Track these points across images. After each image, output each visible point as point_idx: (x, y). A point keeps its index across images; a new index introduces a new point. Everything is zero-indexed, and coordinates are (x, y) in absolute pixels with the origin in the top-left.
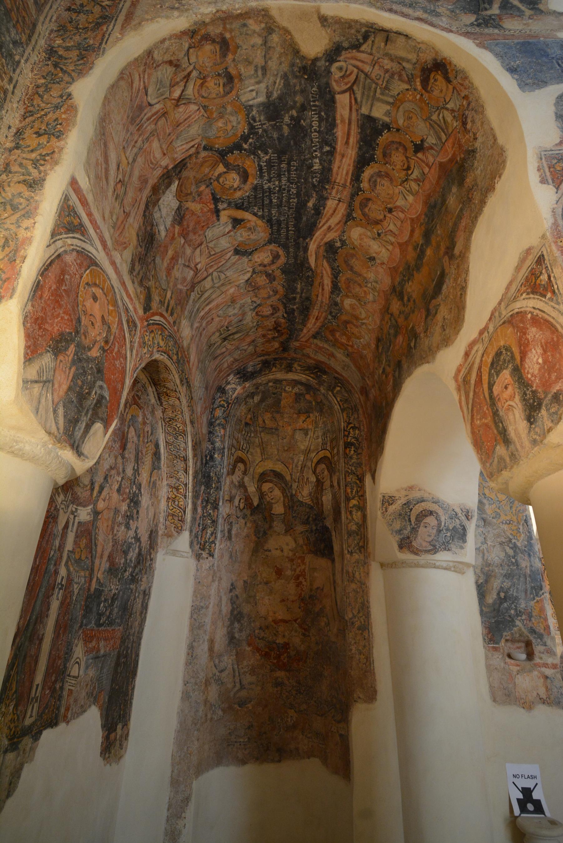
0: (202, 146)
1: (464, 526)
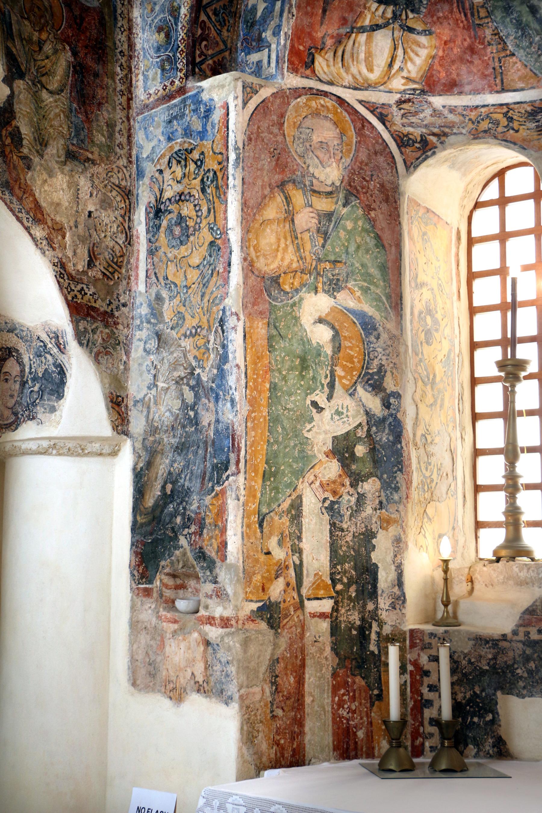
1: (60, 366)
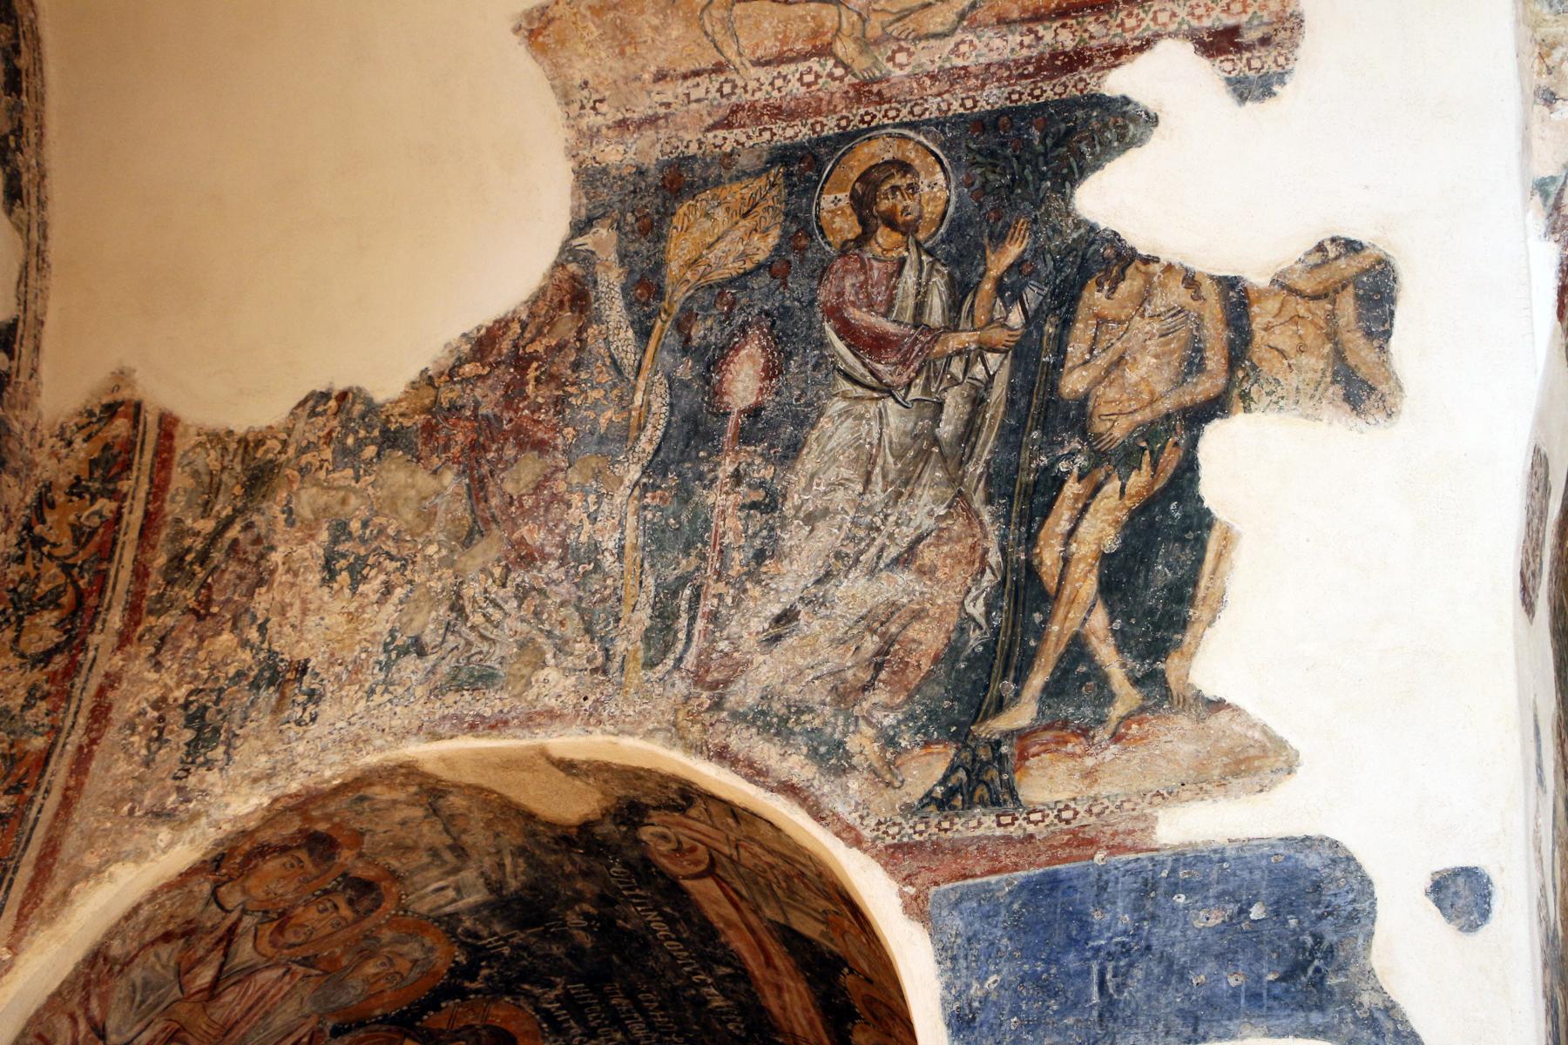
0: (327, 1032)
